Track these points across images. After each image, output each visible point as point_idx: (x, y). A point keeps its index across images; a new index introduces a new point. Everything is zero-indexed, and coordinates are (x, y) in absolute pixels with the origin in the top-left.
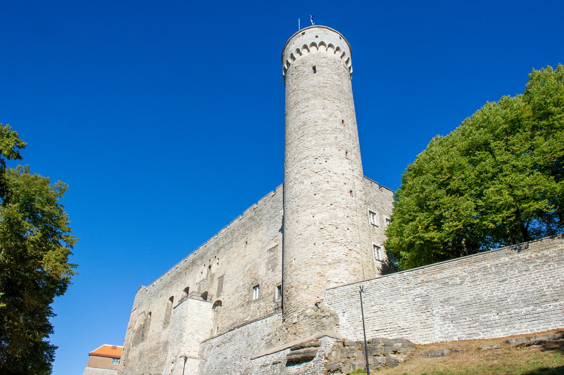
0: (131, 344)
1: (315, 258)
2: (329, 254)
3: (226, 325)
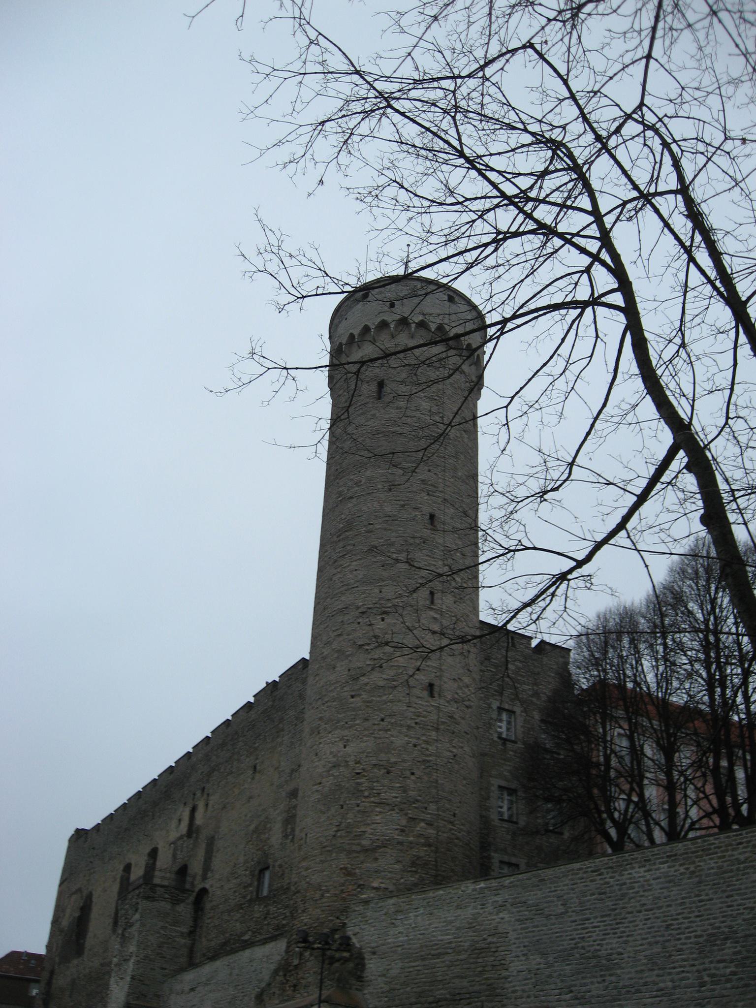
0: (57, 959)
1: (341, 837)
2: (368, 829)
3: (213, 944)
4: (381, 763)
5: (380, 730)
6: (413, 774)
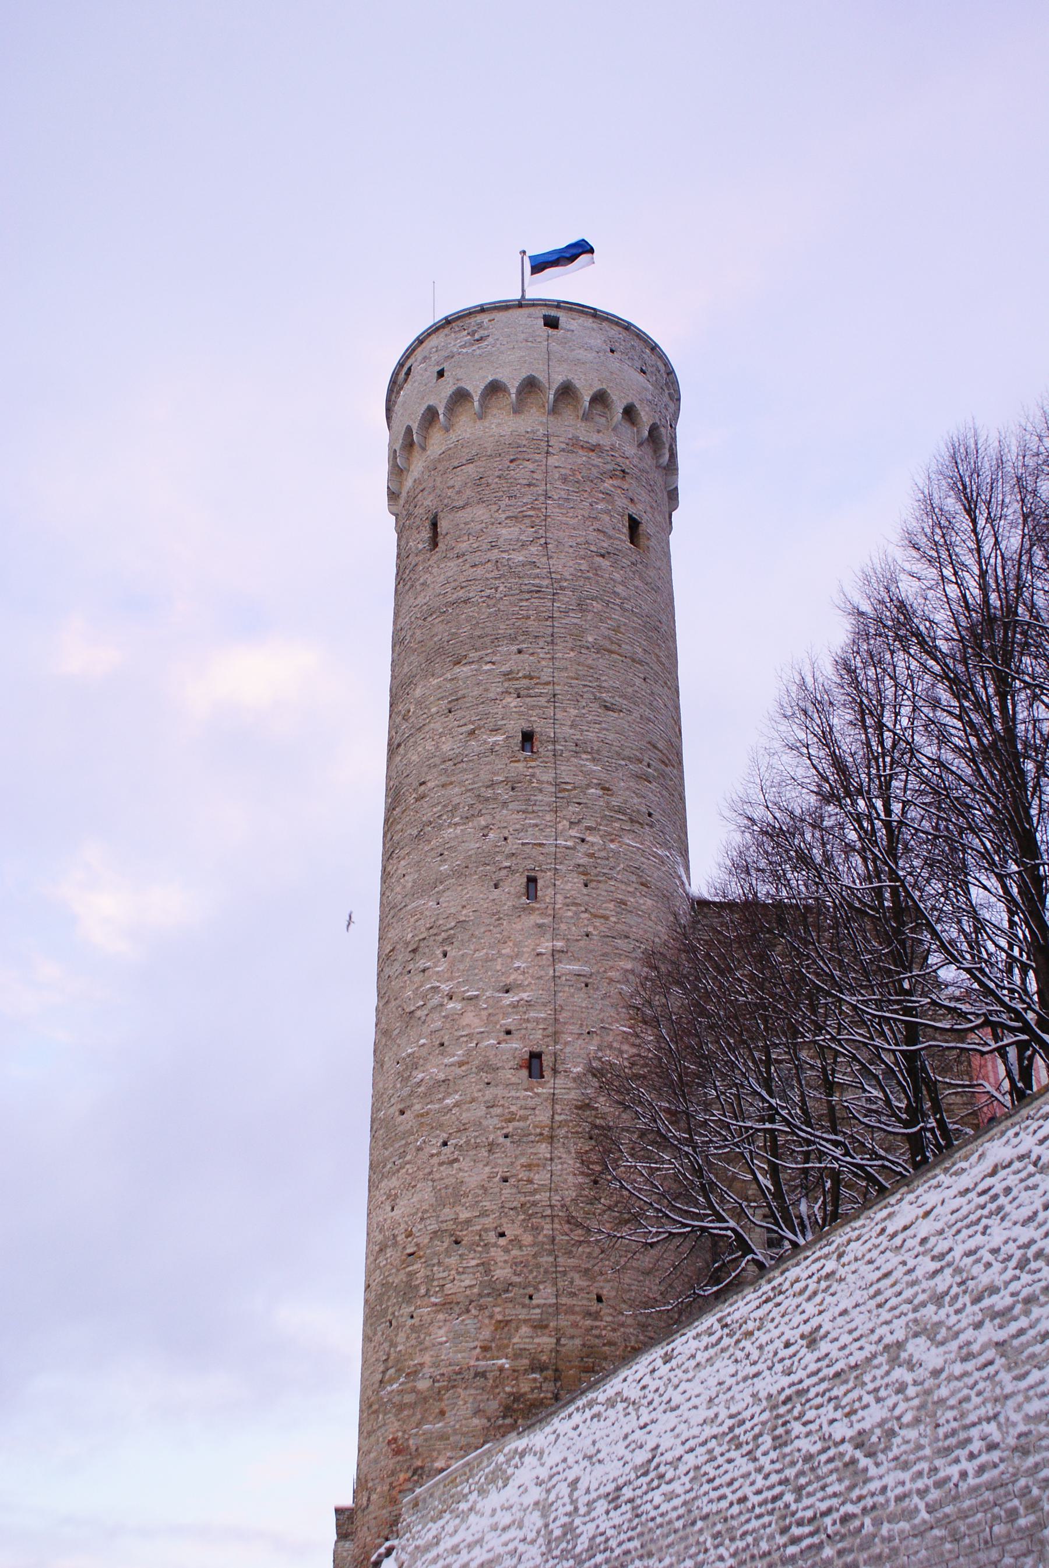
4: (444, 1226)
5: (441, 1164)
6: (502, 1235)
